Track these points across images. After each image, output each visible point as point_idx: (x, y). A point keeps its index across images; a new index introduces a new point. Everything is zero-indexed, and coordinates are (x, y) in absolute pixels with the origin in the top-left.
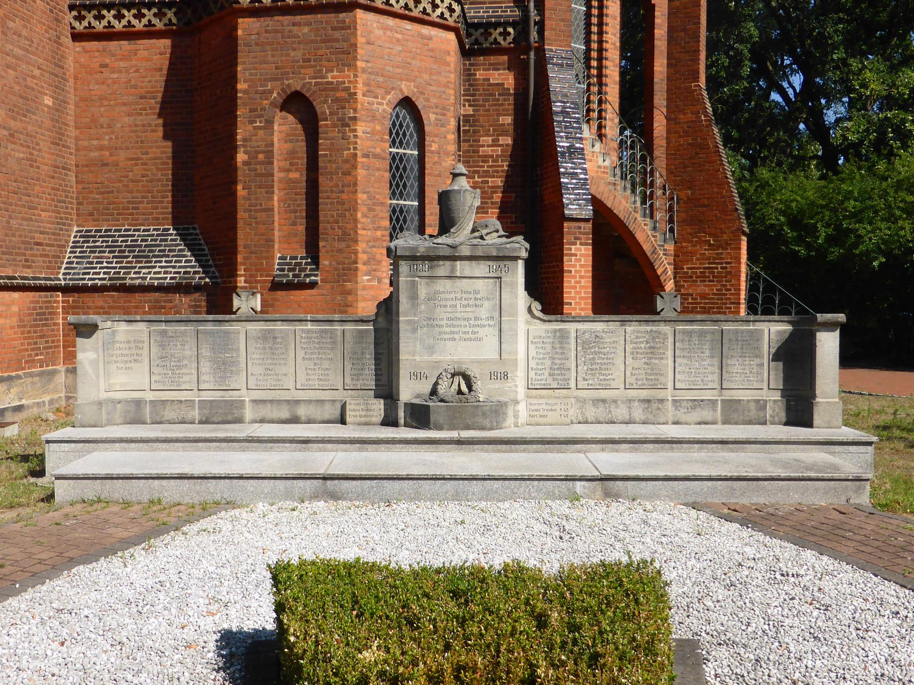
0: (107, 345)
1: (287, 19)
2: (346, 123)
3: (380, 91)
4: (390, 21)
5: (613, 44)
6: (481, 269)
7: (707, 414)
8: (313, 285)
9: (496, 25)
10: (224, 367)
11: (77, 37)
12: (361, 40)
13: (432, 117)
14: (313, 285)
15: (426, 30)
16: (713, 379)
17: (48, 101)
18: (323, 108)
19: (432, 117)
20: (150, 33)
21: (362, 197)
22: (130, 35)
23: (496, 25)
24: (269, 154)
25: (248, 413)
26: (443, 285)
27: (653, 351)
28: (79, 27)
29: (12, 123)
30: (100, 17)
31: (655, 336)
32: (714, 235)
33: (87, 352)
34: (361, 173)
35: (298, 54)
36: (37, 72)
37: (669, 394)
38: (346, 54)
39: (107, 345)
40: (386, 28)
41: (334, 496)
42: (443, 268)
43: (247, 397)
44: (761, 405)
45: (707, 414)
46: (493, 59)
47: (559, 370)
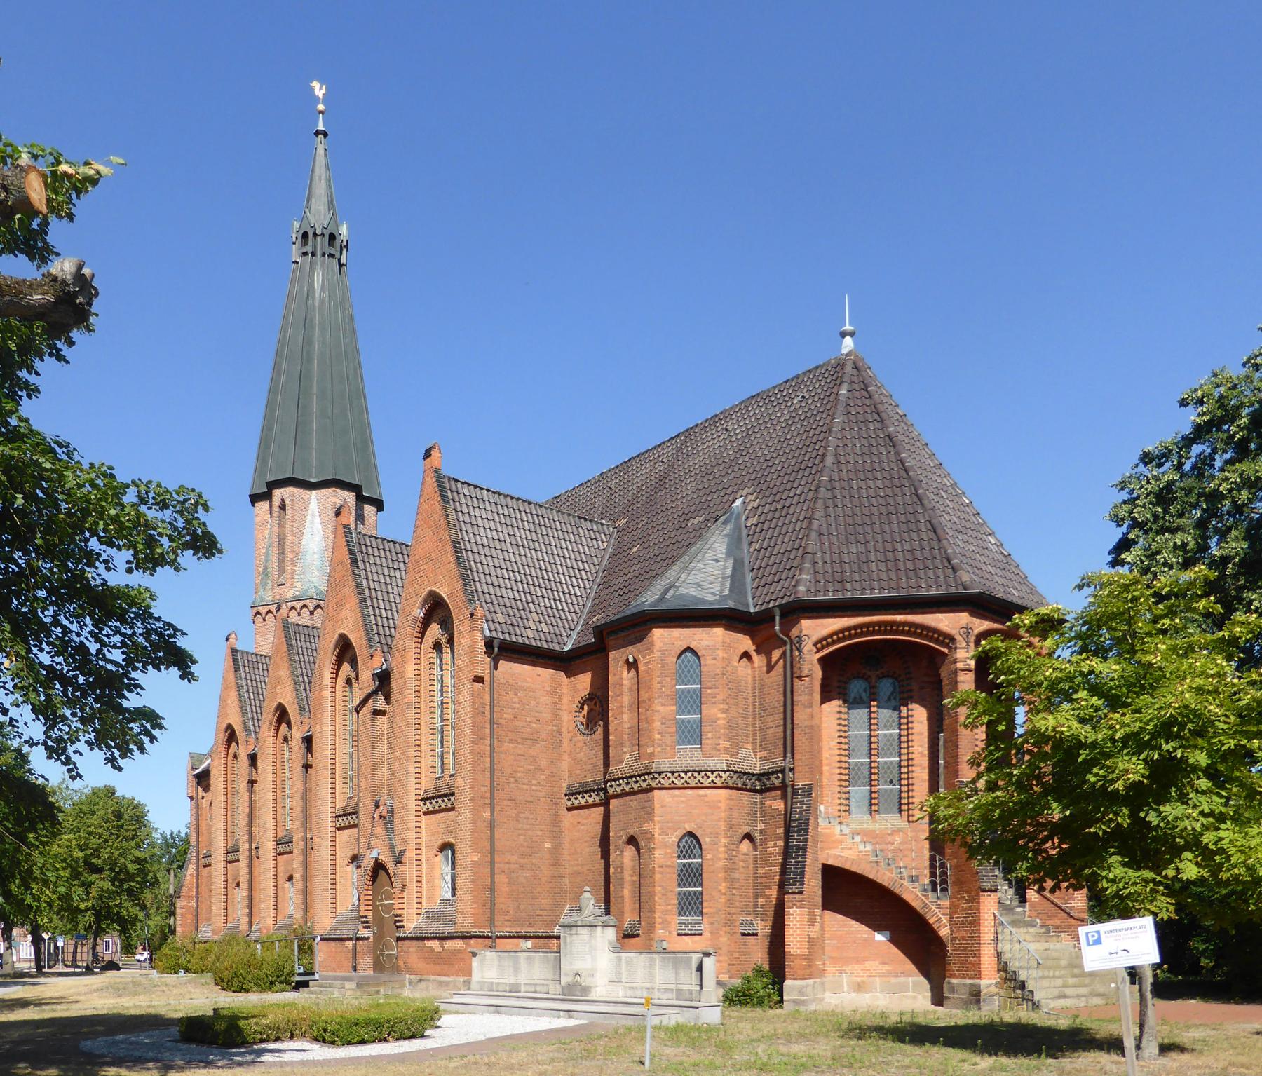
0: (482, 961)
1: (627, 798)
2: (650, 851)
3: (669, 832)
4: (677, 792)
5: (921, 753)
6: (585, 930)
7: (670, 996)
8: (638, 935)
9: (772, 773)
10: (516, 970)
11: (569, 809)
12: (657, 806)
13: (708, 840)
14: (638, 935)
15: (702, 792)
16: (672, 979)
17: (548, 845)
18: (642, 844)
19: (708, 840)
20: (595, 805)
21: (658, 889)
22: (588, 806)
23: (772, 773)
24: (622, 868)
25: (523, 989)
26: (575, 937)
27: (651, 966)
28: (569, 803)
29: (522, 861)
30: (636, 782)
31: (652, 959)
32: (967, 892)
33: (475, 963)
34: (657, 876)
35: (632, 816)
36: (540, 833)
37: (657, 986)
38: (649, 814)
39: (482, 961)
40: (674, 796)
41: (499, 1013)
42: (574, 930)
43: (522, 982)
44: (690, 992)
45: (670, 996)
46: (773, 793)
47: (619, 974)
